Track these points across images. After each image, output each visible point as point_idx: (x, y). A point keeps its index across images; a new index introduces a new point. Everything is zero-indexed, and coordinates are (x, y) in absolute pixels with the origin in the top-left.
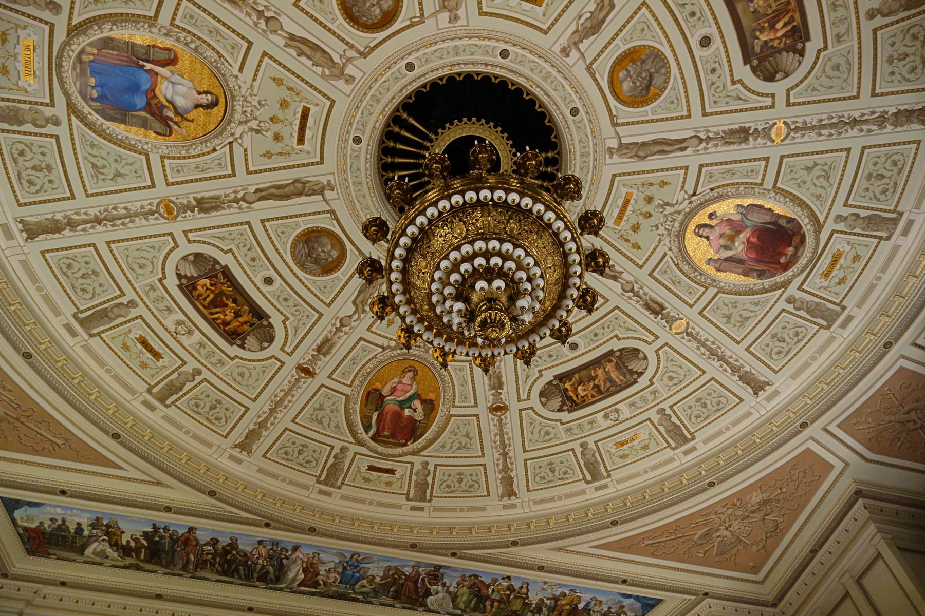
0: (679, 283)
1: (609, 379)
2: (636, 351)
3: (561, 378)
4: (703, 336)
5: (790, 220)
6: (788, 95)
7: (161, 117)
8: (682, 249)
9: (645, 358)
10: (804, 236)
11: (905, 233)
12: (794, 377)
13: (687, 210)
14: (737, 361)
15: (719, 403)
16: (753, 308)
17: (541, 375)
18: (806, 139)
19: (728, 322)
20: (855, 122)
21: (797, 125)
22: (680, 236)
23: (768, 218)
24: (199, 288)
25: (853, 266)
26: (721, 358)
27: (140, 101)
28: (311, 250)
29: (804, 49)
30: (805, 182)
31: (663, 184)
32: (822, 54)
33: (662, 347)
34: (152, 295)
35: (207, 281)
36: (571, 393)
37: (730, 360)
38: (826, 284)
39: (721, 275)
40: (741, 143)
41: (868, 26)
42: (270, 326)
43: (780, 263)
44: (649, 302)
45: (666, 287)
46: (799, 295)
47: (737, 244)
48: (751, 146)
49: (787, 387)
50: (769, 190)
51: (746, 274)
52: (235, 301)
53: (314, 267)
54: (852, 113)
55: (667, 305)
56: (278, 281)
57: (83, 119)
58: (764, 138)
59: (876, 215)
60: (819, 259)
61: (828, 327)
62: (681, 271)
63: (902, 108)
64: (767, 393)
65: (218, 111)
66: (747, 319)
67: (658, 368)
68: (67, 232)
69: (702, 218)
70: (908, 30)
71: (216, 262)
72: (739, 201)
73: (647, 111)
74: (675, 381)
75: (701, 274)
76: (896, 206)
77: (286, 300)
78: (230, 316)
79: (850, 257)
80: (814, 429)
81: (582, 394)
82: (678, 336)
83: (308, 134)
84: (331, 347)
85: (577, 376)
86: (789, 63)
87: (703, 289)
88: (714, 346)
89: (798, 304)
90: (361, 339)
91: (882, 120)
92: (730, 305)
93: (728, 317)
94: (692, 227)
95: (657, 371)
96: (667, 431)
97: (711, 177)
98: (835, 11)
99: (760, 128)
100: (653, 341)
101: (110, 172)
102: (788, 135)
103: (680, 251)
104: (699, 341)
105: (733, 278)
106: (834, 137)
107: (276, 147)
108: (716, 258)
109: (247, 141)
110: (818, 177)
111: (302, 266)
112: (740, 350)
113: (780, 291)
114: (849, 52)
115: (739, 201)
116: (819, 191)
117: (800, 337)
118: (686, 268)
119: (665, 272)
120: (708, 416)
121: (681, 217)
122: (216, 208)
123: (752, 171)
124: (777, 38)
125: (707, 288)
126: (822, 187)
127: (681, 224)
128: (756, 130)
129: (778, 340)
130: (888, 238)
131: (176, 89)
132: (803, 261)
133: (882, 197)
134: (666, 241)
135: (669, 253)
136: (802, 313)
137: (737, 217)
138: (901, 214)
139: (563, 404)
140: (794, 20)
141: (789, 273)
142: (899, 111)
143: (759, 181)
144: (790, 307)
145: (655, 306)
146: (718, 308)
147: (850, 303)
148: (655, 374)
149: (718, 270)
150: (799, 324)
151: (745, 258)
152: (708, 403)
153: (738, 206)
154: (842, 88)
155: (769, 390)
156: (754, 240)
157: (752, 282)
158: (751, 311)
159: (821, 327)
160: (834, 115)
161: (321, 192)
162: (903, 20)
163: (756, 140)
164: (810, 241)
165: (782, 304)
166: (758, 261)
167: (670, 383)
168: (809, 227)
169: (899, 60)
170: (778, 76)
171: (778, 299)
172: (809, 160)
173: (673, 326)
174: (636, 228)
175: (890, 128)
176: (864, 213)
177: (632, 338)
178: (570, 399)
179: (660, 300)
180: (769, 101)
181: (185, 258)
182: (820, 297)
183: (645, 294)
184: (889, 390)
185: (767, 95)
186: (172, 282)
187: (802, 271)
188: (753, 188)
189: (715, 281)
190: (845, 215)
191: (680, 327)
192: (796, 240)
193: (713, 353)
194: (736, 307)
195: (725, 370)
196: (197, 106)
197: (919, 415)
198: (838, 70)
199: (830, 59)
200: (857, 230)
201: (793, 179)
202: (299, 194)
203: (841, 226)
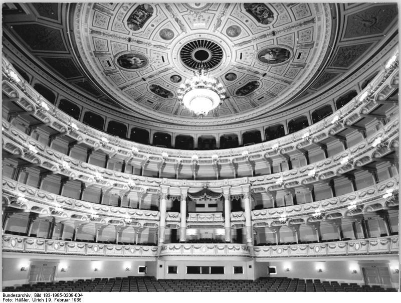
1: (136, 19)
2: (135, 30)
3: (149, 16)
7: (273, 51)
9: (131, 29)
10: (121, 66)
17: (156, 14)
20: (132, 84)
24: (267, 15)
27: (277, 54)
28: (236, 32)
31: (158, 66)
34: (282, 10)
35: (265, 17)
36: (144, 12)
42: (245, 8)
46: (109, 56)
52: (257, 13)
53: (235, 27)
56: (244, 22)
57: (291, 48)
65: (261, 54)
68: (303, 22)
71: (262, 23)
73: (171, 75)
74: (117, 25)
77: (241, 17)
78: (258, 9)
81: (140, 12)
83: (240, 55)
84: (225, 7)
85: (146, 17)
90: (217, 11)
93: (120, 46)
96: (103, 9)
101: (287, 39)
107: (247, 51)
109: (254, 51)
111: (238, 27)
122: (261, 36)
131: (268, 57)
132: (116, 62)
139: (143, 7)
161: (235, 45)
164: (119, 66)
165: (110, 52)
174: (158, 57)
178: (143, 10)
181: (271, 22)
186: (275, 14)
196: (265, 55)
202: (241, 43)
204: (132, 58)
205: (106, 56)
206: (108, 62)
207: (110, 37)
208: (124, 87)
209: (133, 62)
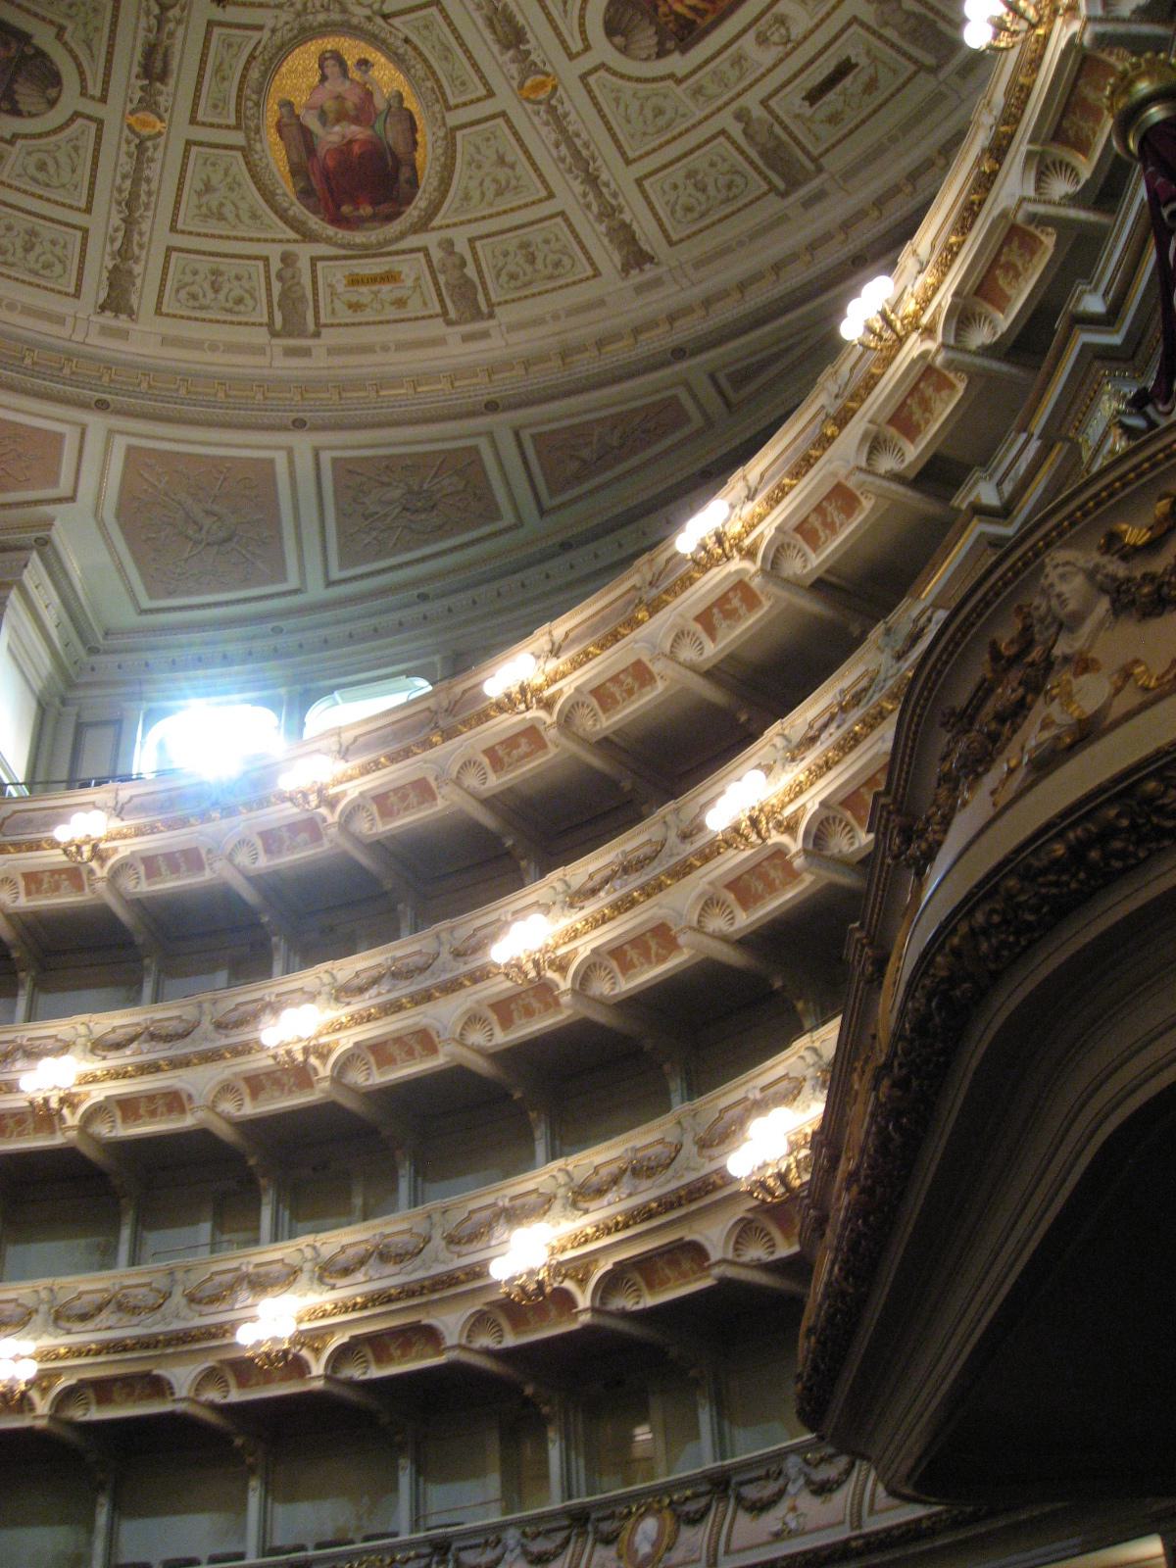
0: (224, 79)
2: (55, 79)
4: (152, 171)
5: (414, 183)
6: (595, 69)
8: (284, 50)
9: (52, 103)
10: (398, 214)
11: (467, 338)
12: (165, 341)
13: (355, 21)
14: (141, 247)
15: (48, 266)
16: (245, 217)
18: (544, 131)
19: (199, 194)
20: (592, 180)
21: (559, 107)
22: (305, 34)
23: (401, 149)
25: (387, 305)
26: (129, 222)
29: (669, 52)
30: (479, 167)
32: (670, 83)
33: (89, 118)
37: (136, 237)
38: (340, 288)
39: (271, 136)
40: (499, 41)
41: (726, 120)
43: (339, 207)
44: (161, 50)
45: (203, 62)
46: (304, 264)
47: (337, 129)
48: (501, 59)
49: (143, 341)
50: (444, 124)
51: (296, 171)
54: (604, 169)
55: (172, 81)
58: (521, 71)
59: (474, 286)
60: (374, 256)
61: (274, 334)
62: (246, 69)
63: (635, 226)
64: (114, 323)
66: (221, 217)
67: (48, 134)
69: (353, 50)
70: (737, 172)
72: (406, 91)
74: (40, 176)
75: (257, 104)
76: (499, 304)
79: (398, 294)
80: (97, 423)
82: (126, 132)
86: (643, 44)
87: (232, 121)
88: (144, 198)
89: (288, 273)
91: (609, 212)
92: (229, 180)
93: (208, 188)
94: (330, 43)
95: (40, 136)
97: (426, 27)
98: (732, 65)
99: (533, 57)
100: (92, 98)
102: (539, 103)
103: (280, 48)
104: (138, 170)
105: (275, 155)
106: (561, 166)
108: (297, 112)
110: (495, 181)
112: (162, 238)
113: (293, 235)
114: (684, 115)
115: (406, 91)
116: (476, 195)
117: (236, 309)
118: (254, 75)
119: (230, 45)
120: (12, 265)
121: (336, 16)
123: (463, 84)
124: (670, 7)
125: (238, 127)
126: (483, 194)
127: (326, 24)
128: (528, 53)
129: (213, 283)
130: (449, 323)
132: (359, 237)
133: (504, 278)
134: (285, 16)
135: (266, 34)
136: (277, 287)
137: (380, 103)
138: (491, 316)
140: (702, 17)
141: (331, 231)
142: (630, 226)
143: (452, 101)
144: (276, 265)
145: (158, 65)
146: (214, 164)
147: (329, 337)
148: (33, 136)
149: (280, 128)
150: (257, 294)
151: (321, 152)
152: (38, 249)
153: (400, 97)
154: (632, 136)
155: (123, 321)
156: (356, 149)
157: (286, 189)
158: (237, 216)
159: (270, 325)
160: (592, 147)
162: (747, 158)
163: (513, 61)
164: (396, 226)
165: (274, 252)
166: (327, 175)
167: (32, 171)
168: (416, 213)
169: (695, 185)
170: (619, 40)
171: (281, 241)
172: (515, 154)
173: (141, 115)
175: (602, 228)
176: (470, 271)
177: (75, 58)
179: (174, 64)
180: (576, 45)
182: (315, 293)
183: (171, 35)
184: (229, 469)
185: (585, 39)
187: (343, 246)
188: (438, 101)
189: (258, 131)
190: (457, 249)
191: (145, 124)
192: (386, 208)
193: (131, 204)
194: (231, 189)
195: (113, 240)
197: (215, 527)
198: (656, 116)
199: (665, 97)
200: (442, 279)
201: (478, 149)
203: (437, 255)
204: (306, 132)
205: (306, 279)
206: (355, 281)
207: (145, 226)
208: (624, 237)
209: (355, 131)
